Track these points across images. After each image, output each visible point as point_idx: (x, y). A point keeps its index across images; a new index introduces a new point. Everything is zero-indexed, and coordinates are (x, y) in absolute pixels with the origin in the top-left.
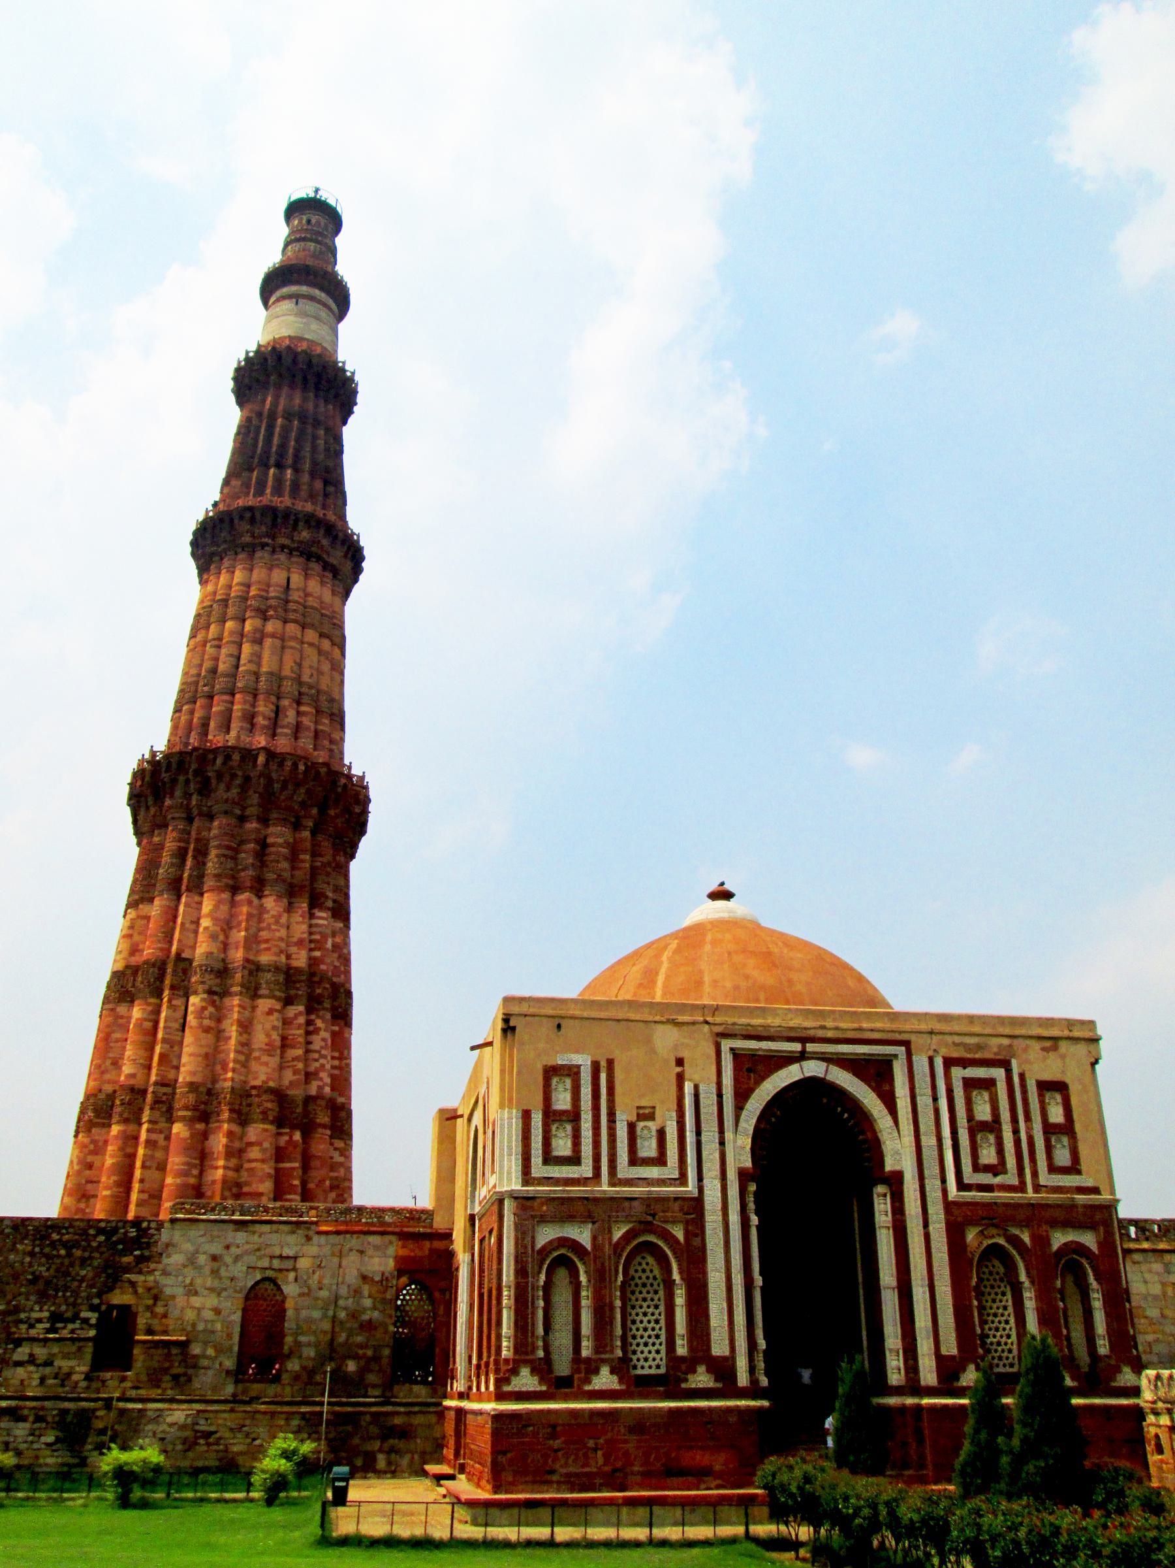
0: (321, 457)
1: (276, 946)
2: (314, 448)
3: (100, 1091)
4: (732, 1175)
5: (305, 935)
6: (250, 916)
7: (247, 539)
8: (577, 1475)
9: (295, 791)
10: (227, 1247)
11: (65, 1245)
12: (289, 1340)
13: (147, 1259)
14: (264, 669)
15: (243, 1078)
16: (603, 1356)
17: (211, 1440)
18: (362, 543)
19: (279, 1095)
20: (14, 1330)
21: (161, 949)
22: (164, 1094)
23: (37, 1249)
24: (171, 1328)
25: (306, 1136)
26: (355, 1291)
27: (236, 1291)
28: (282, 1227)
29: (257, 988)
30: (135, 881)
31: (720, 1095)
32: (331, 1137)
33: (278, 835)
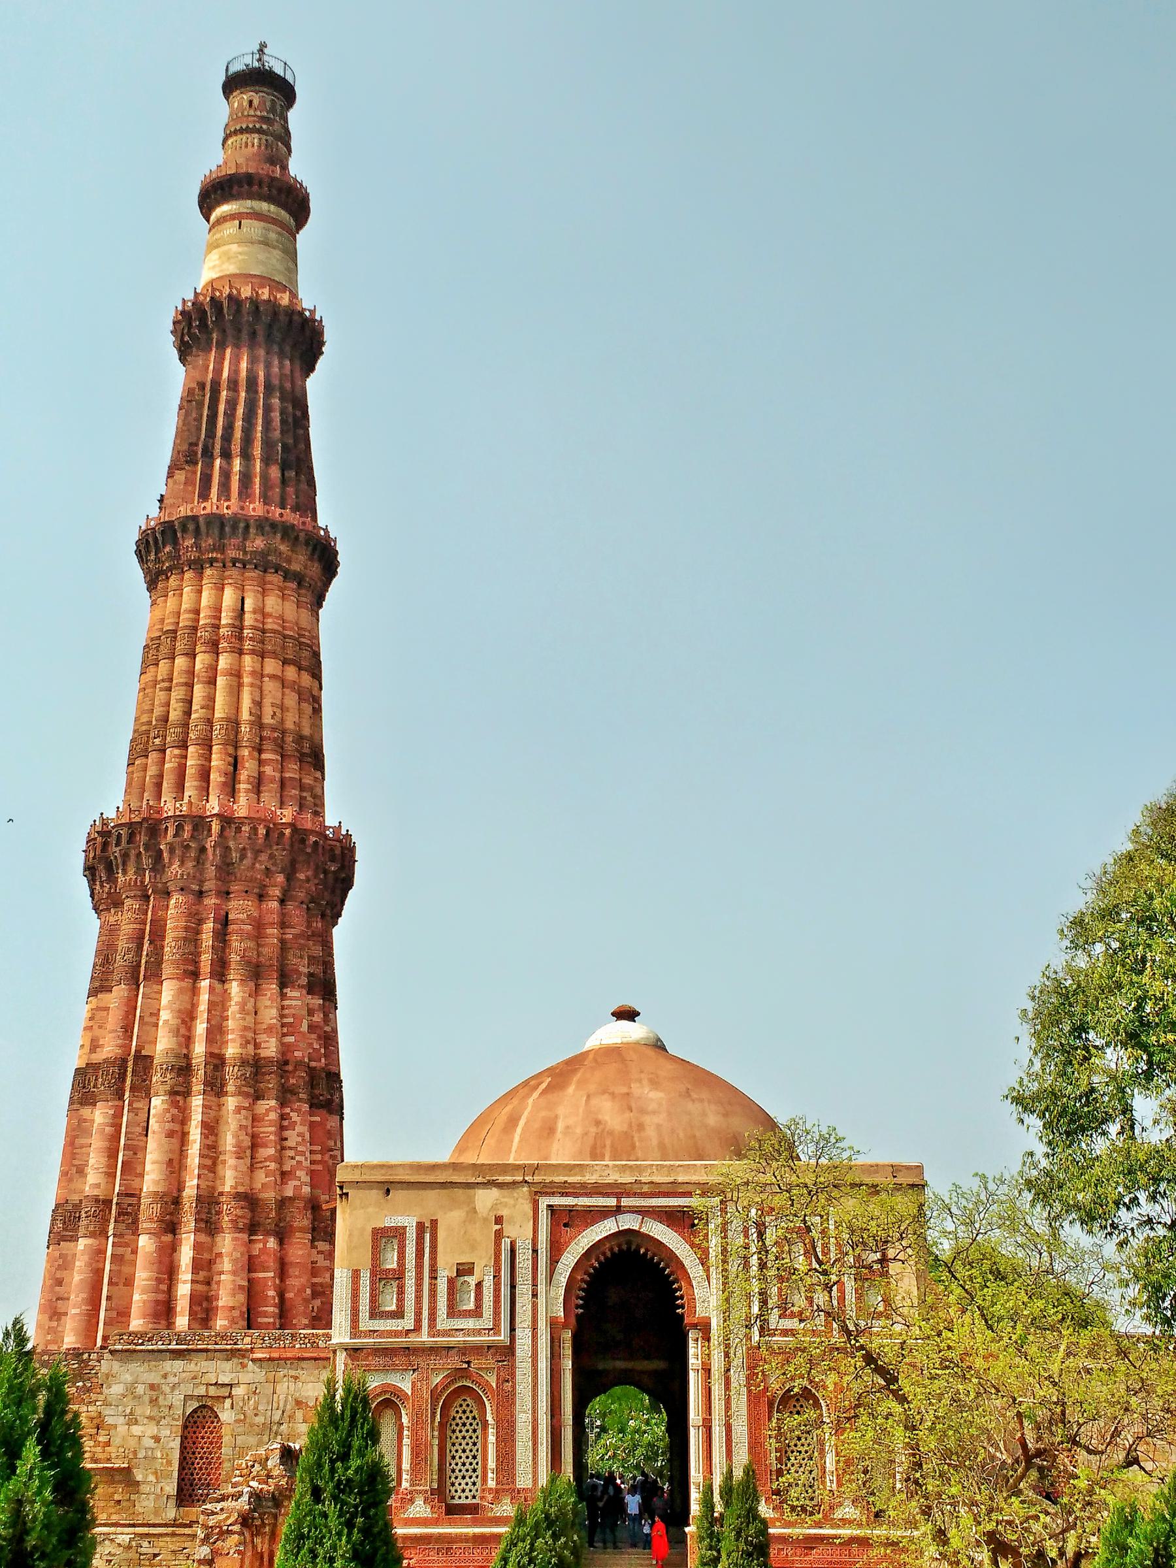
4: (542, 1325)
7: (193, 556)
10: (165, 1376)
13: (89, 1390)
14: (217, 715)
15: (210, 1184)
16: (418, 1488)
19: (249, 1200)
22: (130, 1205)
24: (113, 1455)
25: (281, 1242)
29: (223, 1085)
30: (95, 965)
31: (535, 1251)
32: (313, 1241)
33: (240, 909)
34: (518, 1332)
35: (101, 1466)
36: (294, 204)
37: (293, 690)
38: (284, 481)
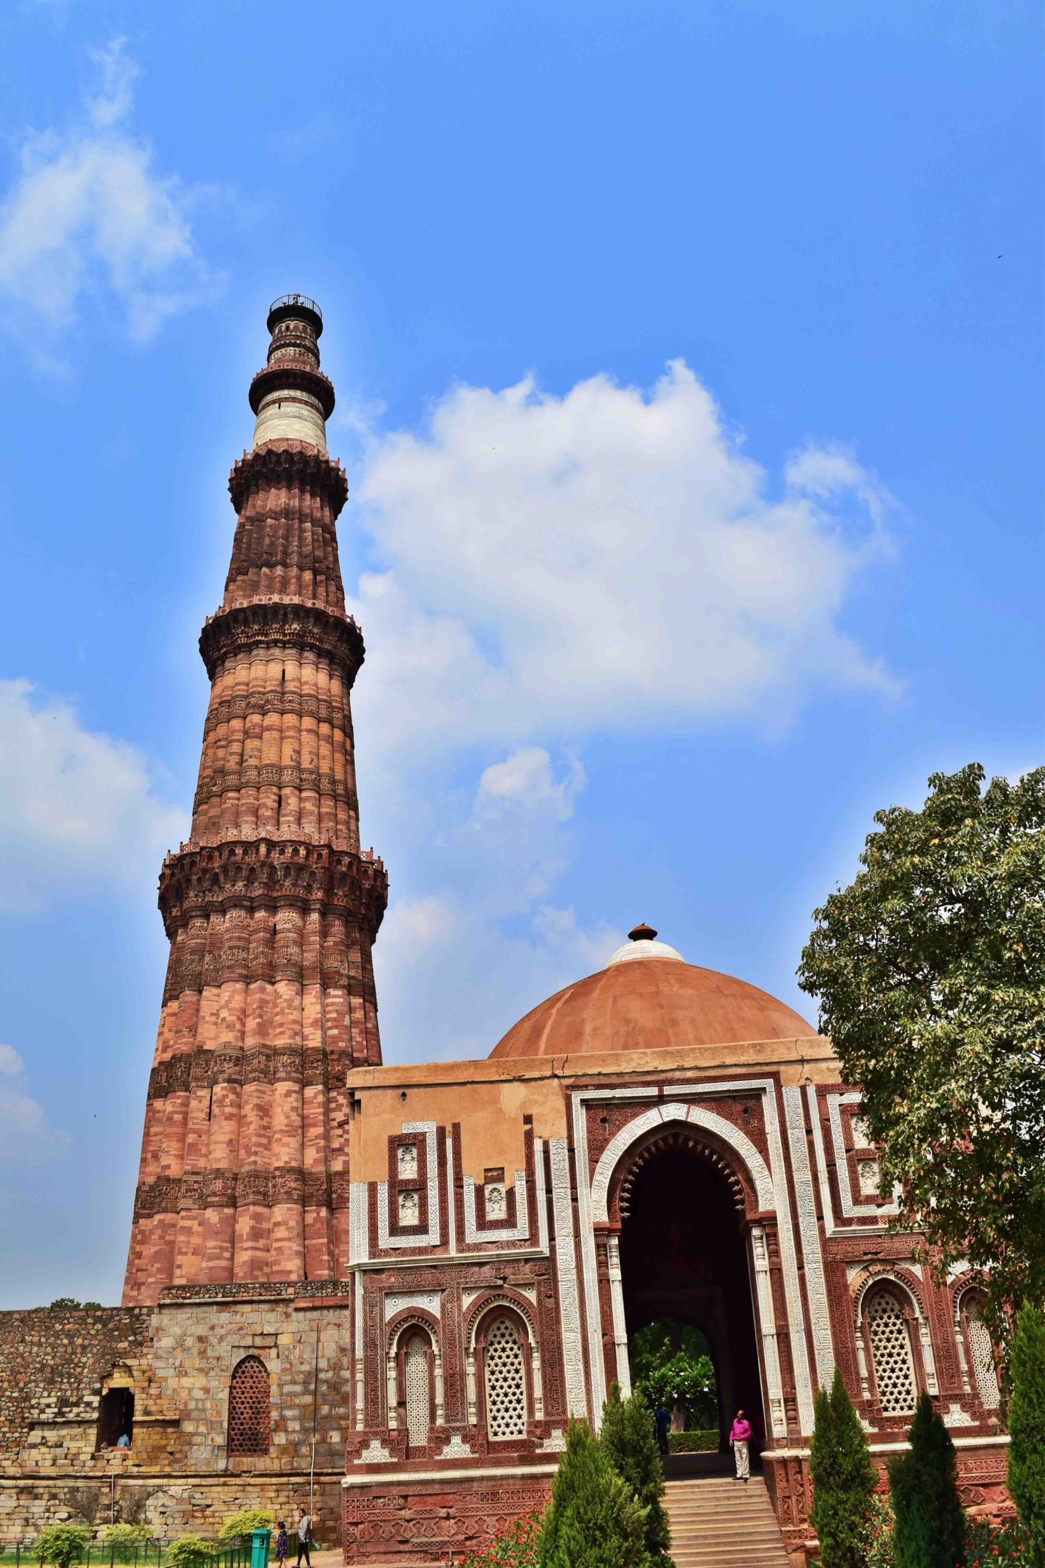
0: (310, 547)
1: (290, 1029)
2: (301, 539)
3: (144, 1184)
5: (319, 1015)
6: (263, 1003)
7: (243, 640)
8: (430, 1544)
9: (298, 876)
10: (212, 1328)
12: (274, 1415)
13: (141, 1344)
15: (267, 1160)
16: (454, 1425)
17: (208, 1512)
18: (358, 624)
19: (301, 1174)
20: (27, 1415)
21: (185, 1044)
22: (195, 1182)
23: (43, 1340)
24: (165, 1408)
25: (332, 1210)
26: (335, 1364)
27: (222, 1370)
28: (264, 1307)
29: (275, 1073)
30: (167, 979)
31: (571, 1150)
33: (286, 919)
34: (559, 1241)
35: (153, 1418)
36: (323, 397)
37: (328, 742)
38: (315, 583)
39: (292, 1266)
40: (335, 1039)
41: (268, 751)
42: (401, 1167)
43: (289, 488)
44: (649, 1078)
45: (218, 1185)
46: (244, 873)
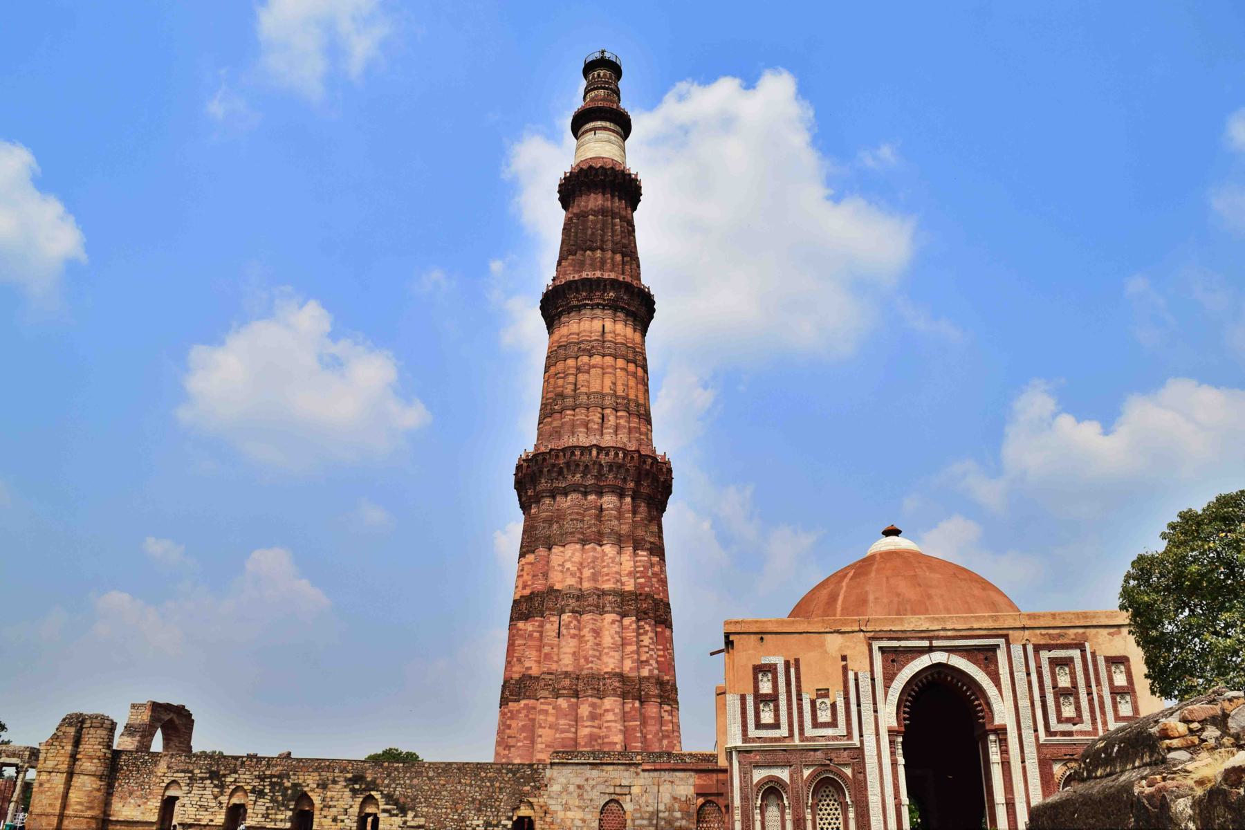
2: (613, 231)
6: (595, 559)
7: (575, 303)
10: (587, 780)
11: (490, 780)
19: (622, 677)
25: (642, 703)
31: (873, 679)
33: (609, 501)
36: (623, 125)
38: (623, 263)
39: (618, 738)
40: (642, 586)
41: (595, 382)
42: (761, 685)
43: (604, 194)
44: (923, 635)
45: (567, 682)
46: (581, 468)
